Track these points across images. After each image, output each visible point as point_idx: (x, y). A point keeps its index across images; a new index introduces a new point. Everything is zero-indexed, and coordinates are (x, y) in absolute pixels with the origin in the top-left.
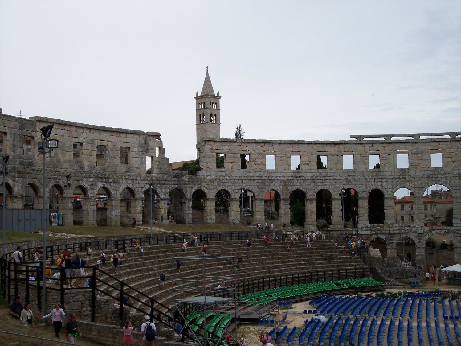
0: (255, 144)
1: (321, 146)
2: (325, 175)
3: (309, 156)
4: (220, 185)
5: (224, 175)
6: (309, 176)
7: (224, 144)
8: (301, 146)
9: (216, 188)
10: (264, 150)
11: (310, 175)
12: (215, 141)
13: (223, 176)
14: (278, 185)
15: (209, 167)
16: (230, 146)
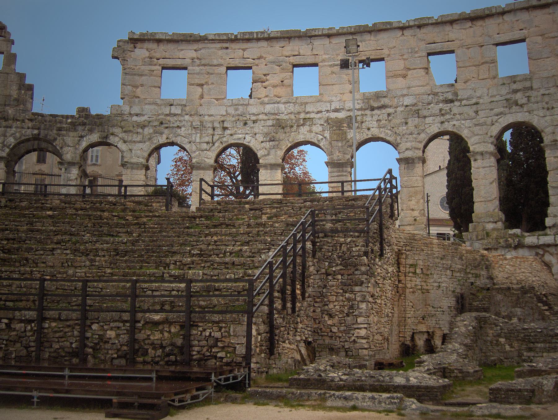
0: (264, 44)
1: (437, 29)
2: (450, 96)
3: (405, 57)
4: (161, 133)
5: (179, 112)
6: (405, 104)
7: (183, 46)
8: (383, 36)
9: (150, 139)
10: (287, 54)
11: (408, 101)
12: (159, 41)
13: (175, 115)
14: (320, 128)
15: (140, 96)
16: (200, 49)
